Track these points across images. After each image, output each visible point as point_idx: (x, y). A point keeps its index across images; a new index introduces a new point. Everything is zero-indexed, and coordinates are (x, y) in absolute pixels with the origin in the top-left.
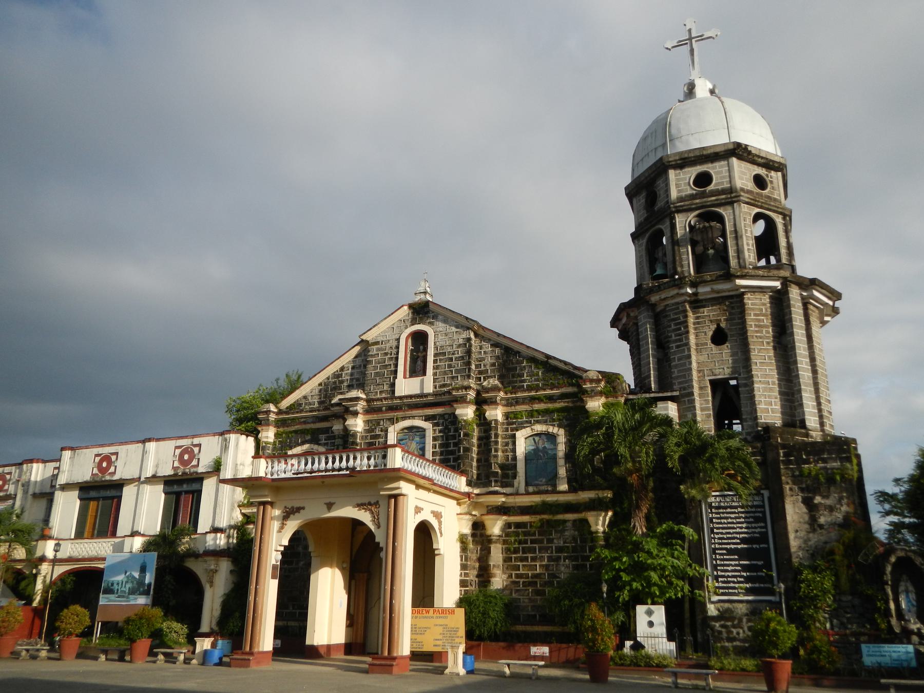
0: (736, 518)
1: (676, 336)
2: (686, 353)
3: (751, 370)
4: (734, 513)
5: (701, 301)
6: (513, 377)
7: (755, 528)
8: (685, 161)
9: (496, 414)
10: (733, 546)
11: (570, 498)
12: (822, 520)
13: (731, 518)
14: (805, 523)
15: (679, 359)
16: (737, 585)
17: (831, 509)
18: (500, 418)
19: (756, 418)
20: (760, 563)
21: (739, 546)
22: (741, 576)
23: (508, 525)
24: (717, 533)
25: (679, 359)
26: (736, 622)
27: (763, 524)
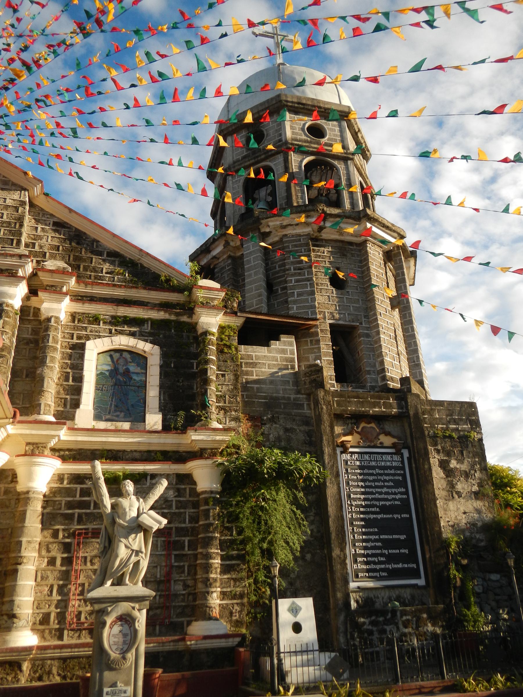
0: (374, 481)
1: (294, 269)
2: (309, 289)
3: (376, 319)
4: (372, 474)
5: (322, 240)
6: (86, 269)
7: (395, 494)
8: (302, 108)
9: (59, 309)
10: (372, 516)
11: (170, 441)
12: (459, 487)
13: (370, 481)
14: (443, 489)
15: (299, 295)
16: (378, 567)
17: (467, 475)
18: (63, 317)
19: (383, 370)
20: (403, 537)
21: (379, 516)
22: (382, 555)
23: (60, 478)
24: (355, 500)
25: (299, 295)
26: (389, 616)
27: (403, 490)
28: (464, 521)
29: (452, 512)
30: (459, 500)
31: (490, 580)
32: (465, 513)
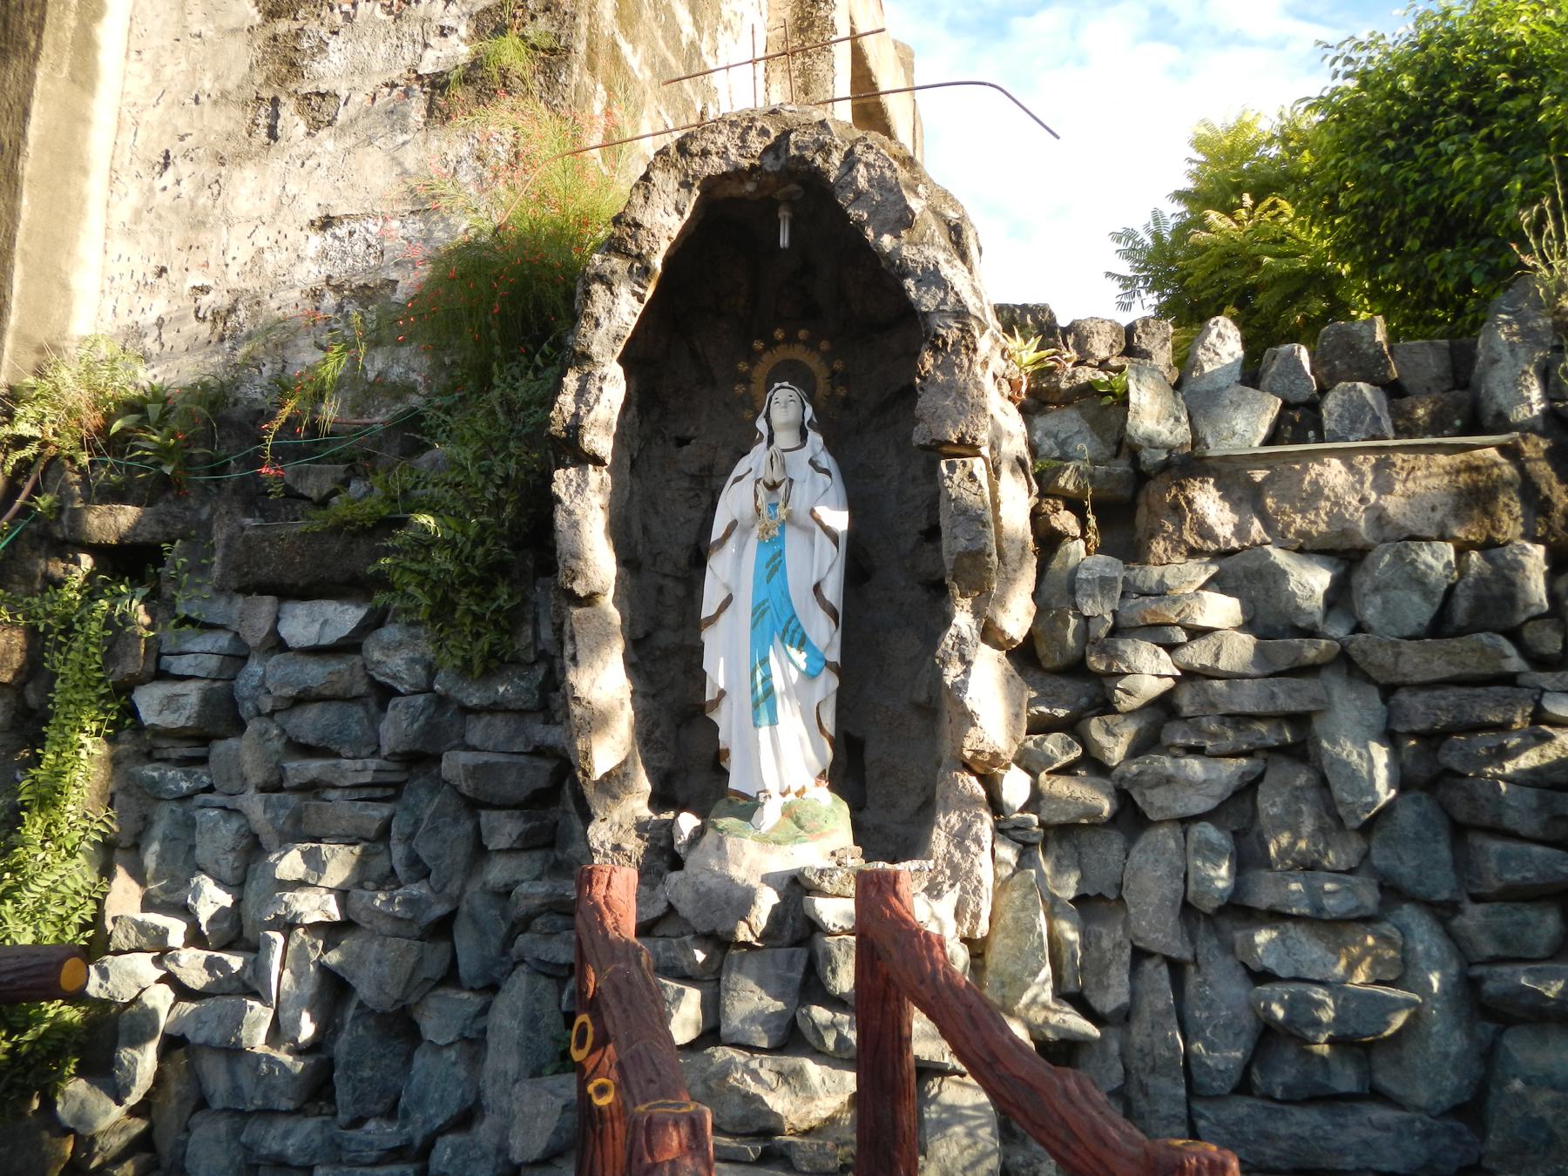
12: (330, 69)
28: (310, 273)
29: (242, 230)
30: (308, 145)
31: (277, 644)
32: (326, 223)
